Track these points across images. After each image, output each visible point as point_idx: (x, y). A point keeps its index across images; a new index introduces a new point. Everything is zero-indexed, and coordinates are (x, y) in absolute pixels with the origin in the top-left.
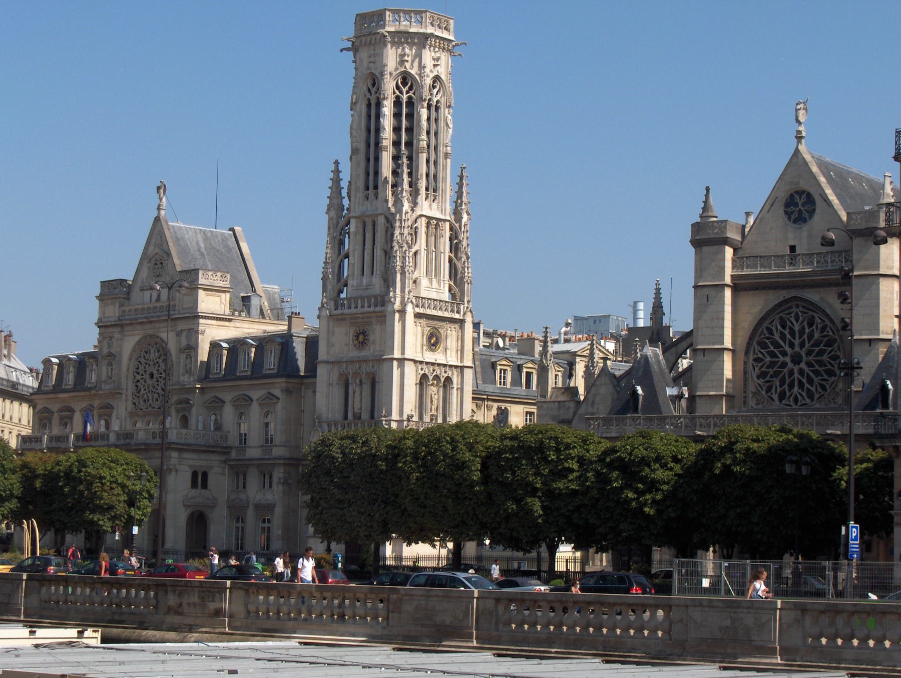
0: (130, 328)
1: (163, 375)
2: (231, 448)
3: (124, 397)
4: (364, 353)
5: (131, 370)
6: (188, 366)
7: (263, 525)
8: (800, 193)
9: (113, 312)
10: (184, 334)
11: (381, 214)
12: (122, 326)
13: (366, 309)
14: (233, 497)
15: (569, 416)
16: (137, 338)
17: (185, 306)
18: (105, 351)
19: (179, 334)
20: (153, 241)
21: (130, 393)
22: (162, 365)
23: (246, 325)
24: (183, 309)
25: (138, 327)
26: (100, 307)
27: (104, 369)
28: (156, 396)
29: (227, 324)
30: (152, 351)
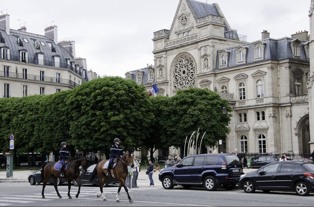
0: (171, 51)
1: (191, 71)
2: (235, 102)
3: (169, 84)
5: (172, 71)
6: (206, 64)
7: (260, 139)
9: (161, 45)
10: (203, 49)
12: (166, 51)
14: (239, 126)
16: (175, 55)
17: (202, 35)
18: (158, 64)
19: (200, 49)
20: (180, 8)
21: (172, 82)
22: (190, 67)
23: (232, 43)
26: (154, 44)
27: (158, 72)
28: (187, 81)
29: (223, 42)
30: (184, 60)
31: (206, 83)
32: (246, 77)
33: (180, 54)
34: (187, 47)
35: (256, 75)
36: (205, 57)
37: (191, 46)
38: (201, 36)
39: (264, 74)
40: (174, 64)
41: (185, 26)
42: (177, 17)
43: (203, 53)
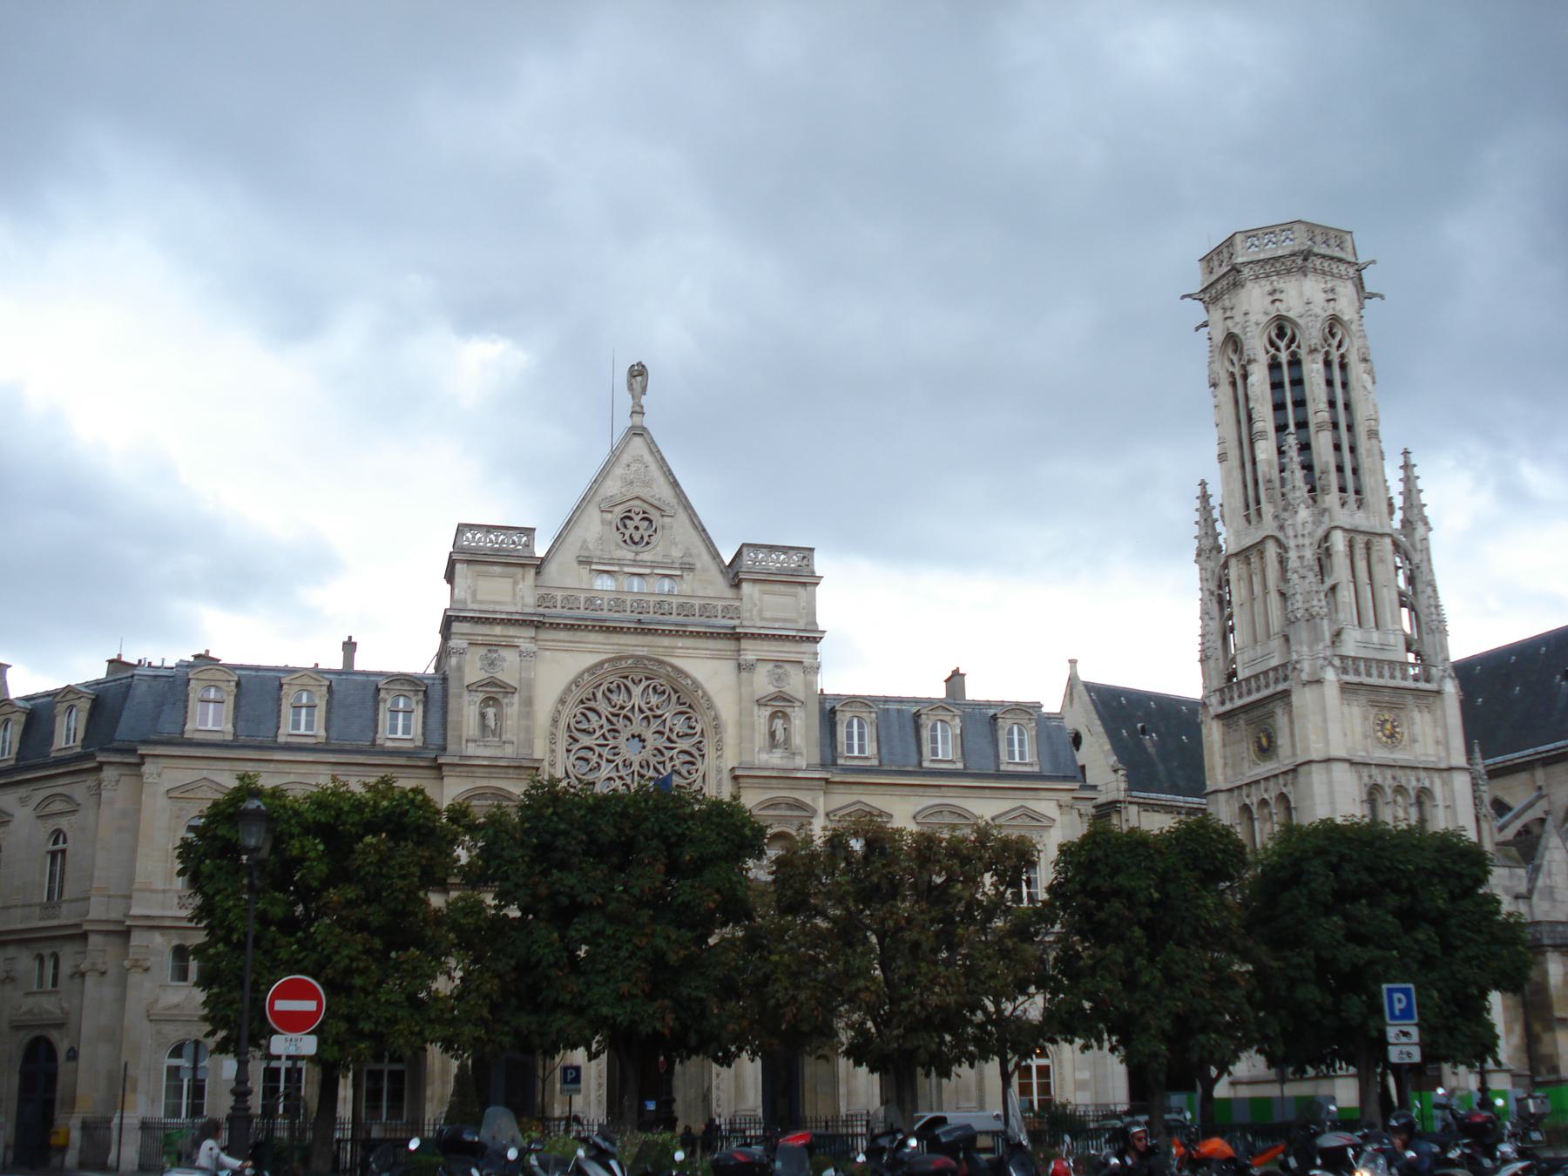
0: (563, 635)
1: (684, 744)
4: (1400, 756)
5: (562, 724)
11: (1390, 535)
13: (1398, 682)
15: (1523, 889)
17: (768, 614)
18: (474, 672)
20: (619, 471)
24: (762, 619)
25: (600, 637)
30: (637, 691)
31: (789, 813)
33: (621, 658)
34: (666, 641)
35: (1014, 822)
36: (779, 705)
37: (690, 642)
38: (762, 619)
39: (1046, 823)
40: (578, 694)
41: (638, 548)
42: (598, 499)
43: (762, 682)
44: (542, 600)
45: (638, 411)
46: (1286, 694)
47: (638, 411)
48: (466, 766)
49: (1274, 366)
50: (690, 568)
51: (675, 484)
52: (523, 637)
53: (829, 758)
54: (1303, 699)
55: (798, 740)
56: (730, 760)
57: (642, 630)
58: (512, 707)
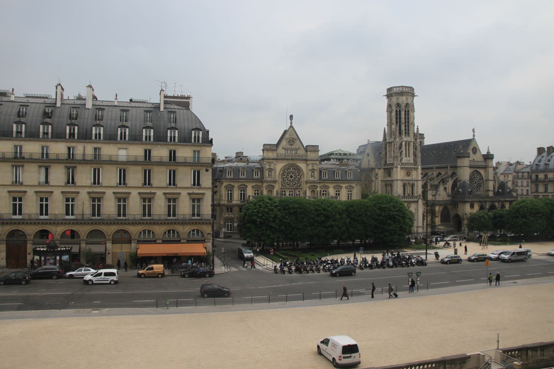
4: (410, 178)
8: (474, 148)
10: (310, 165)
16: (285, 164)
18: (267, 167)
32: (341, 187)
36: (313, 170)
43: (310, 167)
44: (277, 156)
45: (291, 123)
46: (392, 168)
47: (291, 123)
48: (267, 182)
49: (396, 111)
50: (299, 149)
51: (297, 135)
52: (274, 162)
53: (320, 179)
54: (394, 170)
55: (316, 176)
56: (305, 179)
57: (292, 159)
58: (273, 173)
